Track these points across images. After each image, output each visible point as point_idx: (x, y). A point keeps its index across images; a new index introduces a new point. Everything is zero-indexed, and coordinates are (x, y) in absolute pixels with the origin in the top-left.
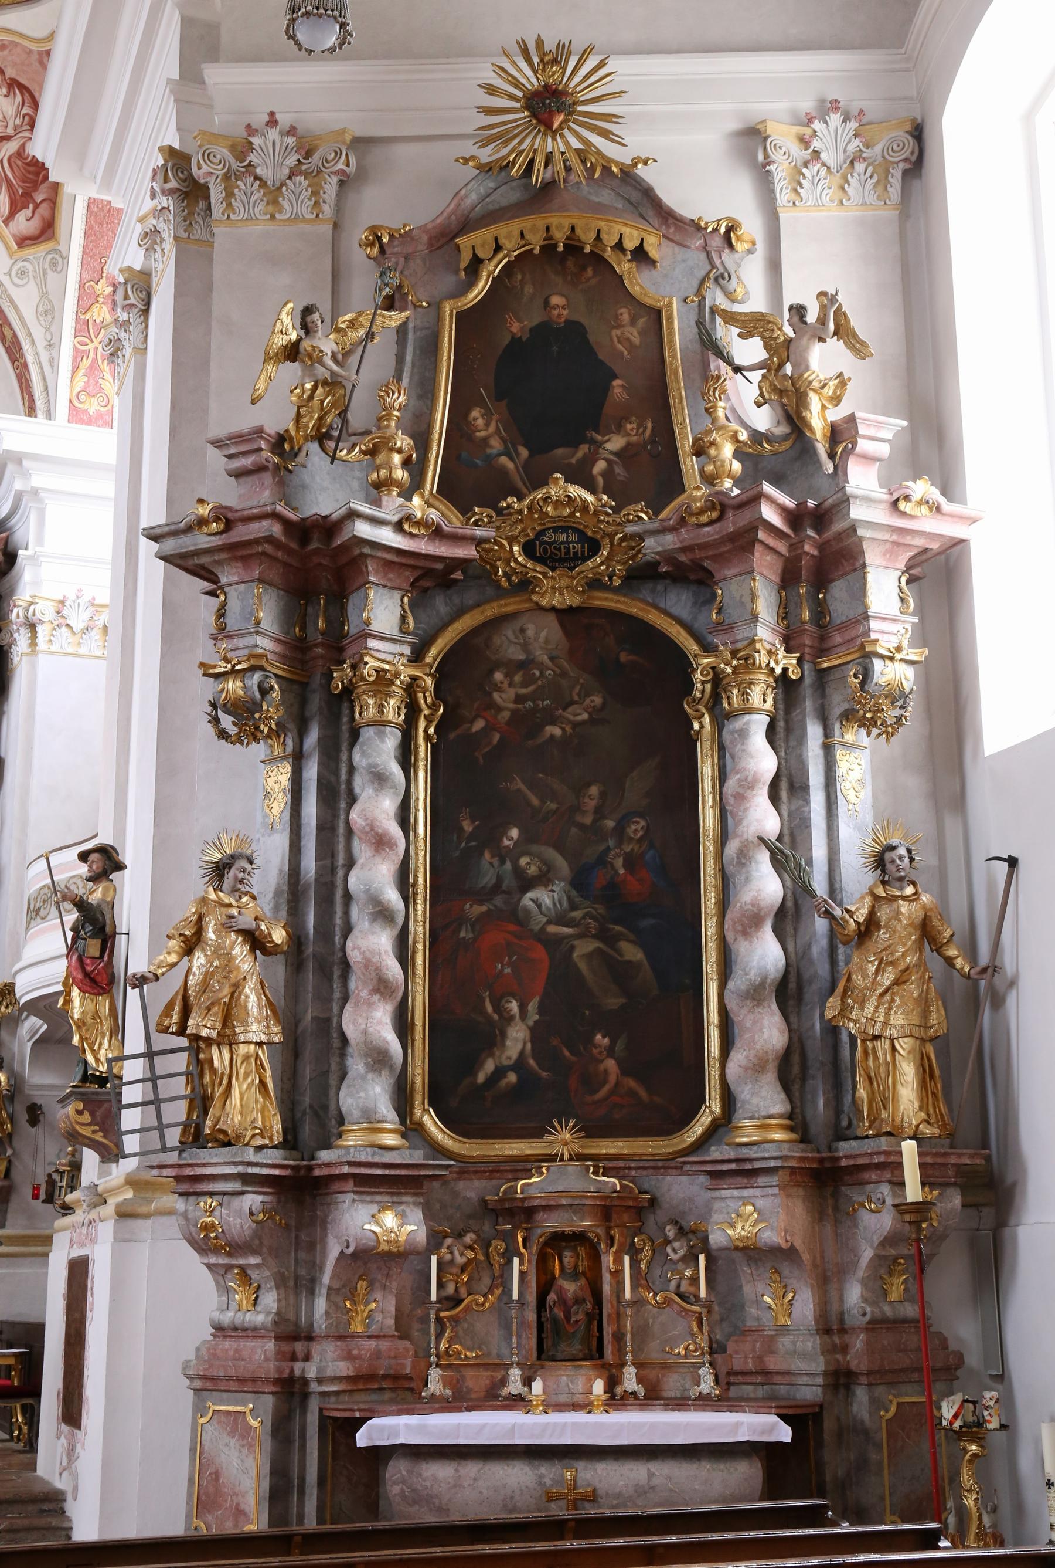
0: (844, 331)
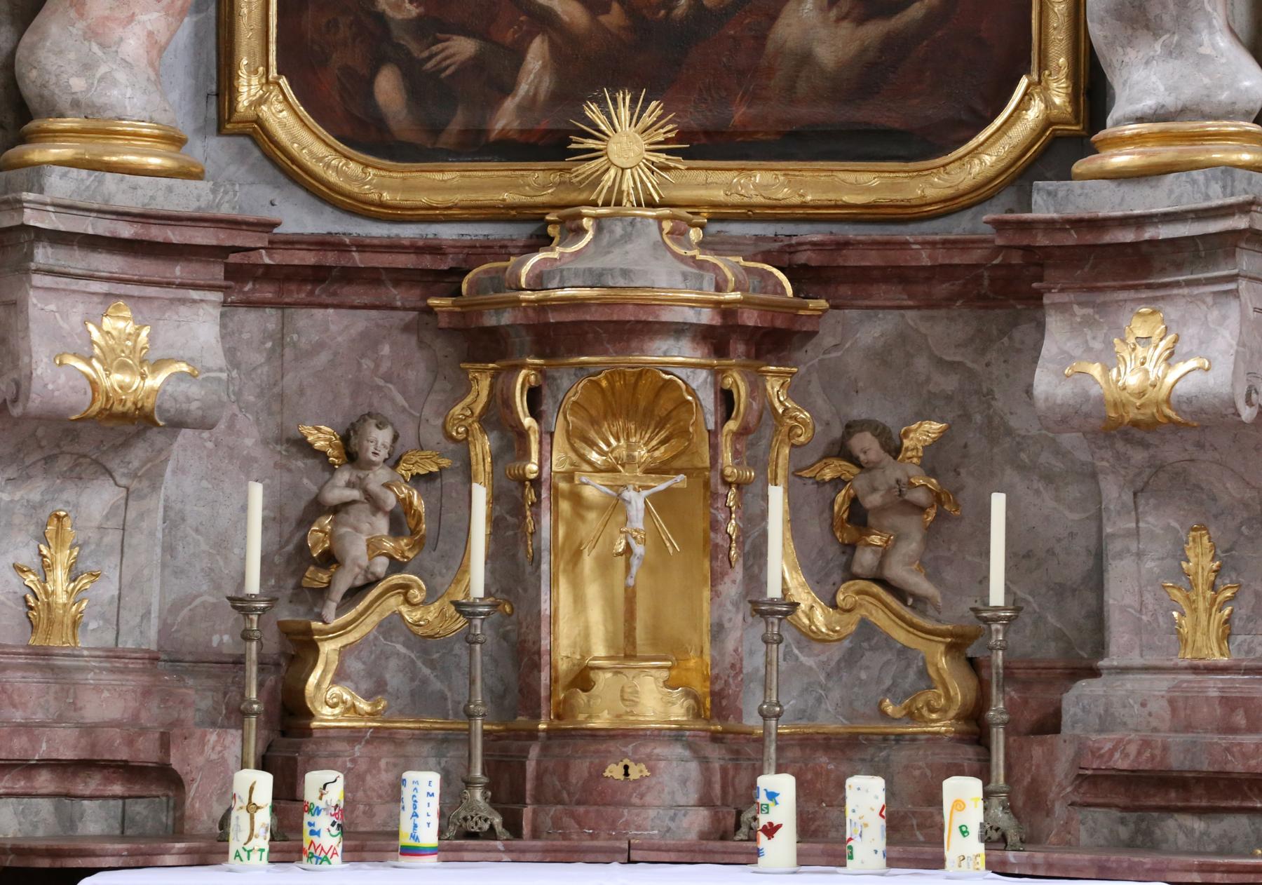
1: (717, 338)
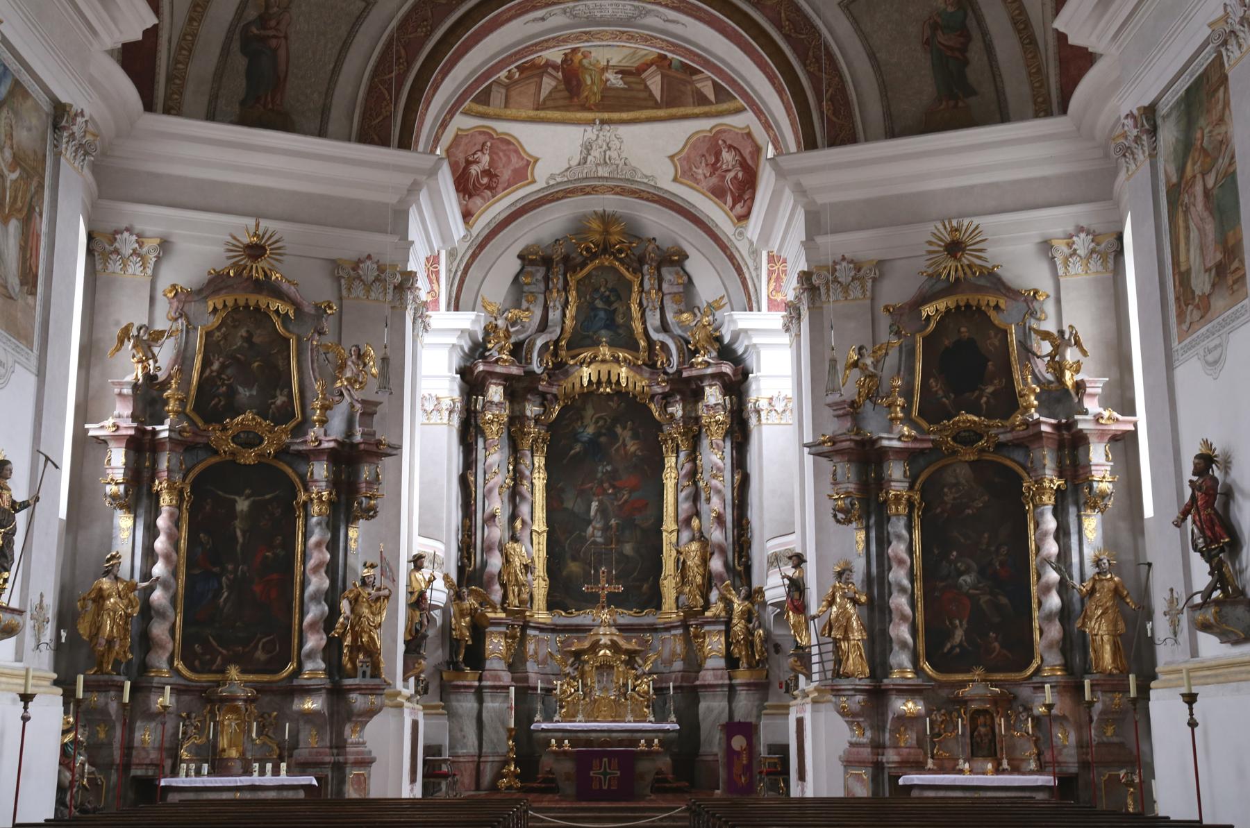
1: (248, 700)
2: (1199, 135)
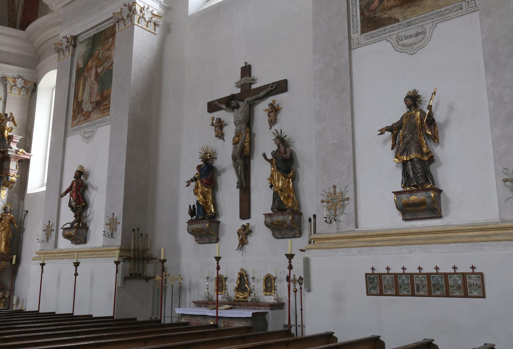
0: (13, 120)
2: (97, 52)
